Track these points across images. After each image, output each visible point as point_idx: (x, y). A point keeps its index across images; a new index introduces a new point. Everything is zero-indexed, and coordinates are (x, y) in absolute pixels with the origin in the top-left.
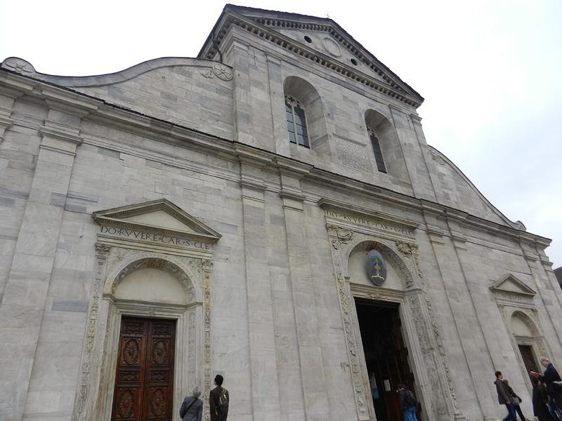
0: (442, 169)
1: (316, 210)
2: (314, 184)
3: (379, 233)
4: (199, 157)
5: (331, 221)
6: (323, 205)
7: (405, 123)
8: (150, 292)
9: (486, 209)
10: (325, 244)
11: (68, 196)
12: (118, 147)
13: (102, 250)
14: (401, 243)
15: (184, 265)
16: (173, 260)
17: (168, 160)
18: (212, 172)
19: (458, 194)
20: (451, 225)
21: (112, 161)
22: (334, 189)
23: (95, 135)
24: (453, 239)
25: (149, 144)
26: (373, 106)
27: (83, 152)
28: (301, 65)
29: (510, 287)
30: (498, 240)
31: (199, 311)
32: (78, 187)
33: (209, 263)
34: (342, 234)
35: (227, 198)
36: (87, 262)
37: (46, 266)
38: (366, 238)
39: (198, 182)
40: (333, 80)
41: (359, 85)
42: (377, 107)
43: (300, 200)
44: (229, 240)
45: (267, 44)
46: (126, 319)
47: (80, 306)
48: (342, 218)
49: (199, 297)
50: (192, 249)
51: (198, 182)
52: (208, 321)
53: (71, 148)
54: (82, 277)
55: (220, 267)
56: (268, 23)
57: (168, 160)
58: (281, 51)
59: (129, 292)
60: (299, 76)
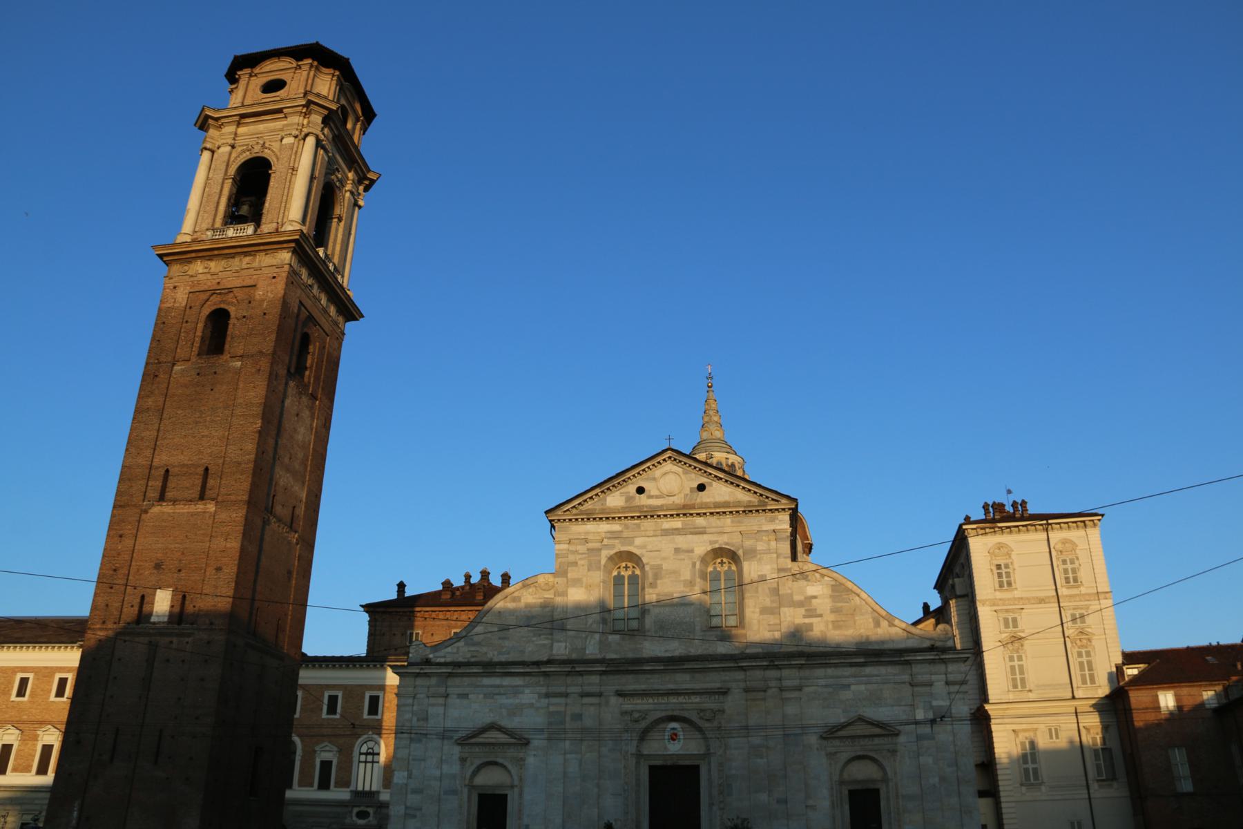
0: (812, 590)
1: (614, 700)
4: (518, 681)
6: (620, 694)
7: (760, 546)
8: (490, 779)
12: (467, 690)
13: (463, 760)
14: (702, 710)
15: (506, 763)
16: (500, 760)
17: (497, 691)
18: (527, 691)
19: (832, 617)
20: (786, 672)
21: (465, 702)
23: (456, 686)
24: (781, 689)
25: (486, 681)
26: (716, 542)
27: (450, 701)
28: (625, 534)
30: (868, 670)
31: (516, 790)
32: (449, 724)
33: (523, 760)
34: (636, 715)
36: (456, 769)
37: (438, 773)
38: (664, 714)
40: (666, 533)
41: (700, 521)
42: (722, 541)
43: (600, 695)
44: (537, 742)
45: (591, 527)
46: (480, 796)
49: (516, 782)
52: (521, 794)
53: (441, 701)
55: (531, 760)
57: (497, 691)
58: (604, 527)
59: (480, 780)
60: (623, 549)
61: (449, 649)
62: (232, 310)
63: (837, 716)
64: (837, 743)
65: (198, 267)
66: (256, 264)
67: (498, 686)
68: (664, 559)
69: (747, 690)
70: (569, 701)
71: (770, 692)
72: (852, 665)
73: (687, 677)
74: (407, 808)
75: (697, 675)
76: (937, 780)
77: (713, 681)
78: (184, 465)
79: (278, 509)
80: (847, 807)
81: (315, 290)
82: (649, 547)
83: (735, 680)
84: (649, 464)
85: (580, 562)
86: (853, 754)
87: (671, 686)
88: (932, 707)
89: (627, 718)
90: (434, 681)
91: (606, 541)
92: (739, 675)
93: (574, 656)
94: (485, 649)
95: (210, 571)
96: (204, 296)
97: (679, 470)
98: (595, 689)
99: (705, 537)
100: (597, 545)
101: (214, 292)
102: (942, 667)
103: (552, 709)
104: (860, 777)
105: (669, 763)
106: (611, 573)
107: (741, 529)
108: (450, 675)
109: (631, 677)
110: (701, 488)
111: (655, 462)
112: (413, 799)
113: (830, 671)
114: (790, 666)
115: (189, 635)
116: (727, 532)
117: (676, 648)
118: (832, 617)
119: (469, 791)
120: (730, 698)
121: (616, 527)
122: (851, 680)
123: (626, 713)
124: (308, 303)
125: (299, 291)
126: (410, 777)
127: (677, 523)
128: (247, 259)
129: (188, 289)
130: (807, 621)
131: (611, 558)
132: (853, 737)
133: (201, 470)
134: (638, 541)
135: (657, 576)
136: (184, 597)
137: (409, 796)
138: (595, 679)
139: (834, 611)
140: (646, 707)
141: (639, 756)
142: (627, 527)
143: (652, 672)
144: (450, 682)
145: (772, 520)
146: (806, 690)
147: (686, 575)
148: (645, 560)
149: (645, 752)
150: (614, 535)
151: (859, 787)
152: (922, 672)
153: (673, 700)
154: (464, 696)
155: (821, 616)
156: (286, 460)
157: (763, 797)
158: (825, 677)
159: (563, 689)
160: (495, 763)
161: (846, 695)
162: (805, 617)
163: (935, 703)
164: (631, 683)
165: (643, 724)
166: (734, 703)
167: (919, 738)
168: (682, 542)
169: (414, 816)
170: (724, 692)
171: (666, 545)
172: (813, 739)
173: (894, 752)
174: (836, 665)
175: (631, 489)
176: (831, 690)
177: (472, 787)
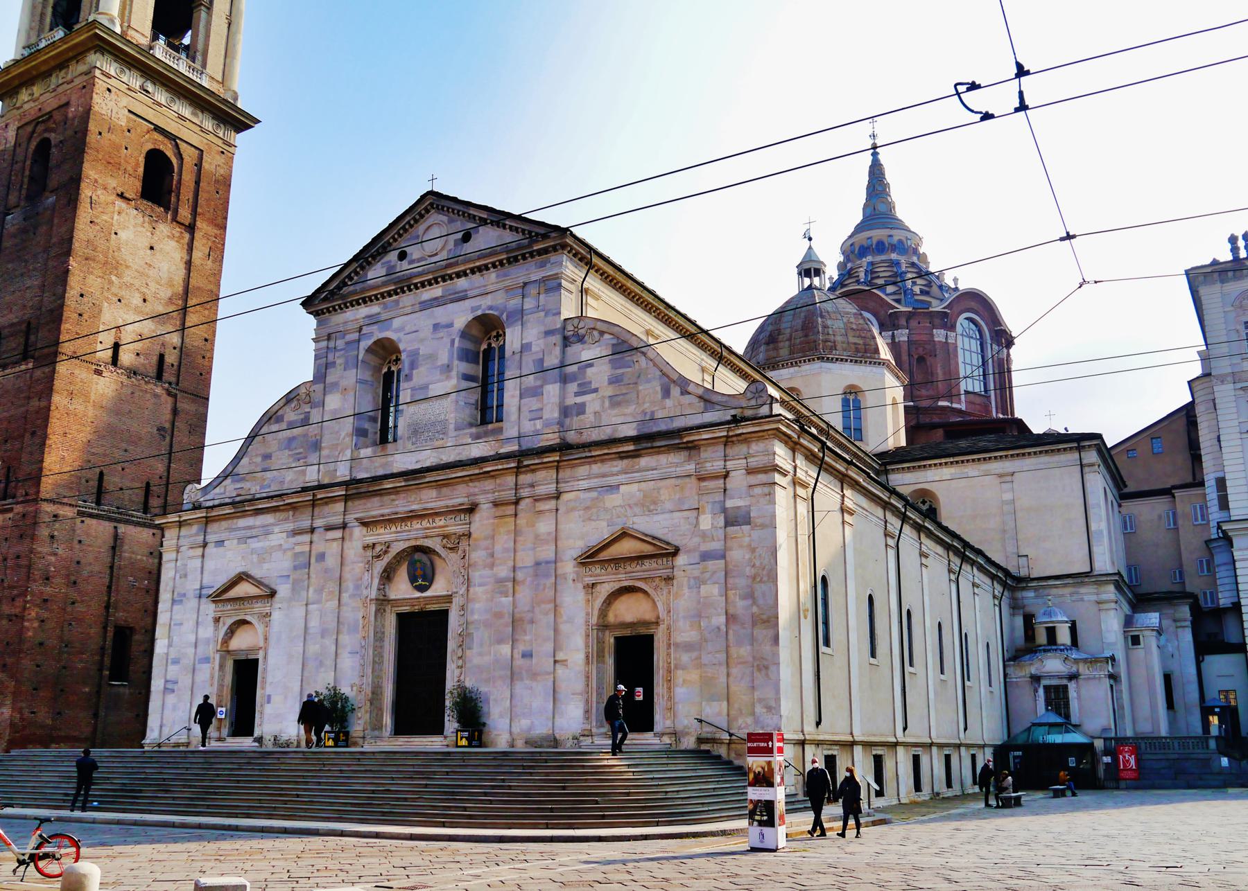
0: (587, 353)
2: (360, 498)
3: (421, 534)
4: (268, 519)
5: (370, 540)
6: (365, 524)
7: (529, 304)
9: (666, 393)
10: (359, 567)
11: (202, 588)
12: (223, 536)
13: (217, 620)
14: (445, 536)
16: (248, 618)
17: (249, 533)
18: (276, 529)
19: (608, 391)
20: (541, 475)
22: (381, 495)
23: (216, 532)
25: (242, 522)
26: (479, 307)
27: (207, 550)
28: (384, 317)
29: (627, 547)
30: (644, 461)
33: (268, 615)
35: (285, 551)
36: (207, 631)
37: (192, 638)
38: (407, 544)
39: (267, 543)
41: (462, 283)
42: (484, 305)
44: (283, 590)
47: (206, 660)
48: (382, 531)
50: (259, 607)
51: (267, 543)
54: (207, 641)
55: (276, 616)
56: (351, 279)
57: (249, 533)
58: (363, 311)
61: (217, 490)
62: (52, 136)
63: (599, 531)
64: (597, 570)
65: (24, 96)
66: (69, 77)
67: (250, 528)
68: (422, 341)
69: (496, 504)
70: (316, 537)
71: (523, 505)
72: (622, 456)
73: (433, 493)
74: (166, 681)
75: (444, 490)
76: (723, 619)
77: (458, 496)
78: (12, 325)
79: (126, 357)
80: (610, 661)
81: (162, 96)
82: (408, 329)
83: (484, 492)
84: (408, 218)
85: (339, 361)
86: (617, 586)
87: (414, 507)
88: (724, 510)
89: (369, 553)
90: (195, 528)
91: (364, 331)
92: (488, 484)
93: (326, 481)
94: (246, 485)
95: (28, 435)
96: (29, 129)
97: (445, 219)
98: (338, 520)
99: (467, 304)
100: (355, 336)
101: (36, 122)
102: (741, 449)
103: (298, 549)
104: (629, 618)
105: (416, 609)
106: (381, 369)
107: (507, 283)
108: (208, 521)
109: (376, 500)
110: (467, 237)
111: (415, 214)
112: (173, 671)
113: (596, 468)
114: (545, 466)
115: (11, 510)
116: (488, 293)
117: (428, 458)
118: (608, 391)
119: (223, 659)
120: (477, 517)
121: (374, 309)
122: (622, 478)
123: (368, 546)
124: (149, 114)
125: (125, 101)
126: (170, 645)
127: (437, 291)
128: (62, 73)
129: (17, 124)
130: (579, 400)
131: (369, 350)
132: (617, 561)
133: (24, 327)
134: (397, 323)
135: (413, 366)
136: (9, 468)
137: (171, 668)
138: (340, 507)
139: (615, 381)
140: (387, 538)
141: (383, 602)
142: (385, 307)
143: (395, 491)
144: (213, 527)
145: (543, 265)
146: (565, 497)
147: (443, 358)
148: (401, 347)
149: (392, 597)
150: (374, 320)
151: (627, 632)
152: (713, 460)
153: (416, 525)
154: (220, 543)
155: (596, 390)
156: (137, 300)
157: (506, 649)
158: (589, 477)
159: (306, 523)
160: (244, 622)
161: (613, 500)
162: (577, 394)
163: (730, 504)
164: (374, 508)
165: (387, 559)
166: (481, 522)
167: (706, 556)
168: (441, 314)
169: (173, 691)
170: (472, 509)
171: (424, 321)
172: (568, 567)
173: (669, 579)
174: (602, 459)
175: (393, 256)
176: (594, 494)
177: (226, 652)
